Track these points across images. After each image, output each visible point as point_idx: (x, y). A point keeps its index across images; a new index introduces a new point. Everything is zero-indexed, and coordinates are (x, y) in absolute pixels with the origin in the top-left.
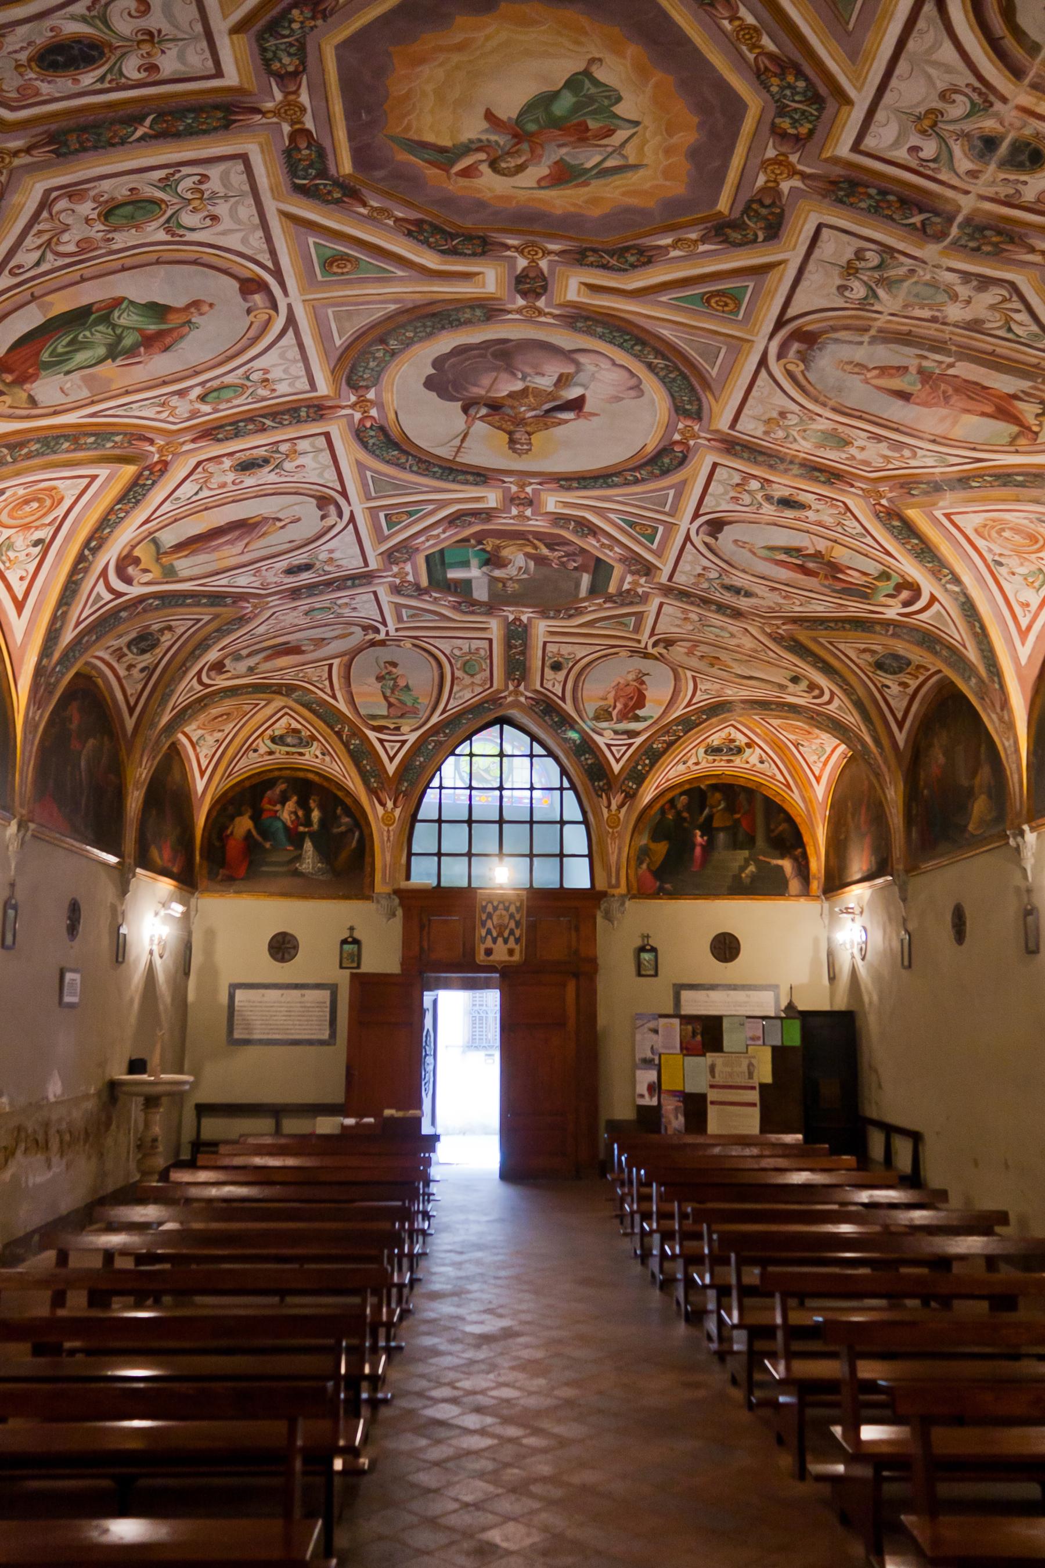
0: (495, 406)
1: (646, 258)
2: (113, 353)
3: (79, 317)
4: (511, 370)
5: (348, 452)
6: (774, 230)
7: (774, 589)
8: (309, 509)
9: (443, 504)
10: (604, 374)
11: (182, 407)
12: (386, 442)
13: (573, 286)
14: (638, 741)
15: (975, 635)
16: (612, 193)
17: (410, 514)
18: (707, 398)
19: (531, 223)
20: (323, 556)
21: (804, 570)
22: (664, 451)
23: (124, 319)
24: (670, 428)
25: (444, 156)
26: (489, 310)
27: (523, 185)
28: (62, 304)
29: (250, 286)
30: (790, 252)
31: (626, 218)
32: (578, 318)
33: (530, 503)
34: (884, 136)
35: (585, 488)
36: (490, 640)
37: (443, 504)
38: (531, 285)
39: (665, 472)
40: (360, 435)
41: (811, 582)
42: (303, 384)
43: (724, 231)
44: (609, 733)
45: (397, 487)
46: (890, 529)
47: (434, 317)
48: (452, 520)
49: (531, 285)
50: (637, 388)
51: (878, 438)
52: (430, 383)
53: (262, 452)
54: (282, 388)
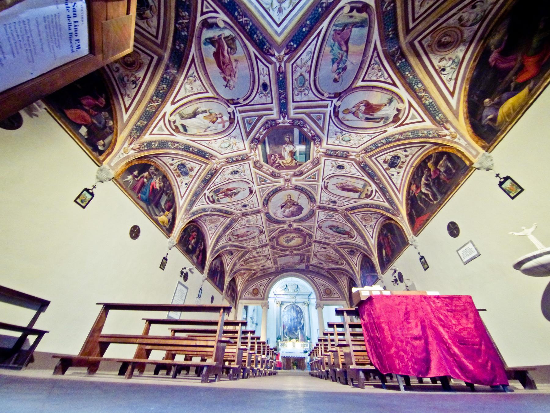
0: (294, 204)
1: (279, 232)
2: (338, 228)
3: (338, 233)
4: (292, 212)
5: (318, 198)
6: (270, 240)
7: (229, 179)
8: (330, 187)
9: (303, 180)
10: (279, 214)
11: (336, 217)
12: (311, 199)
13: (286, 226)
14: (199, 19)
15: (199, 210)
16: (284, 236)
17: (310, 178)
18: (266, 218)
19: (291, 232)
20: (333, 169)
21: (228, 190)
22: (267, 204)
23: (335, 230)
24: (268, 209)
25: (299, 237)
26: (295, 221)
27: (292, 235)
28: (339, 235)
29: (320, 228)
30: (268, 239)
31: (283, 234)
32: (284, 222)
33: (286, 180)
34: (267, 249)
35: (277, 188)
36: (293, 102)
37: (303, 180)
38: (290, 226)
39: (265, 199)
40: (315, 202)
41: (225, 187)
42: (320, 213)
43: (274, 237)
44: (222, 25)
45: (312, 187)
46: (229, 212)
47: (301, 220)
48: (301, 174)
49: (290, 226)
50: (275, 214)
51: (245, 225)
52: (302, 209)
53: (331, 204)
54: (323, 213)
